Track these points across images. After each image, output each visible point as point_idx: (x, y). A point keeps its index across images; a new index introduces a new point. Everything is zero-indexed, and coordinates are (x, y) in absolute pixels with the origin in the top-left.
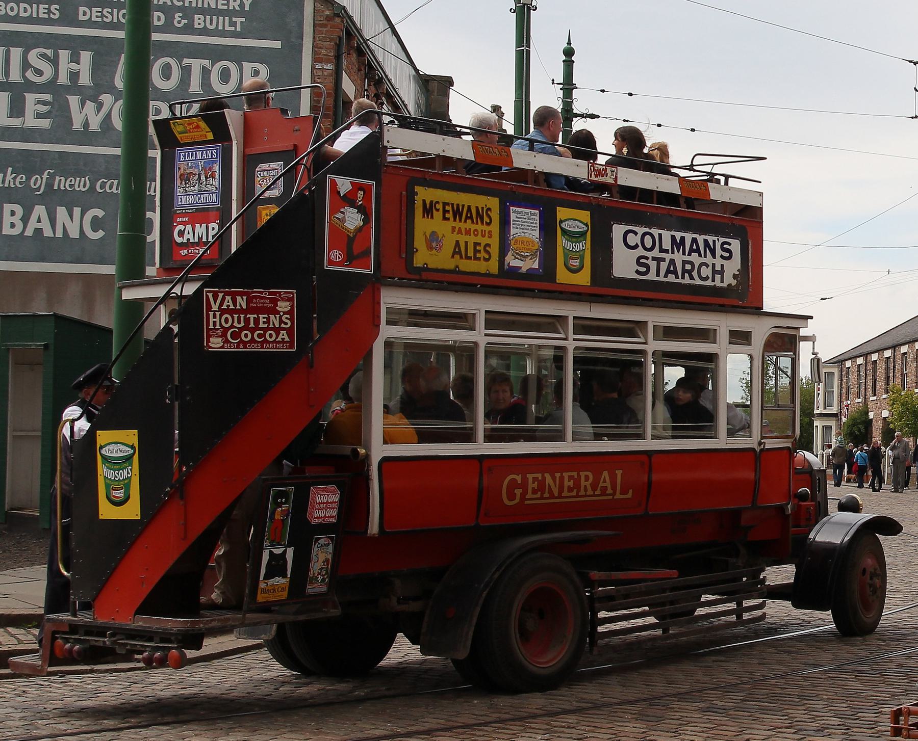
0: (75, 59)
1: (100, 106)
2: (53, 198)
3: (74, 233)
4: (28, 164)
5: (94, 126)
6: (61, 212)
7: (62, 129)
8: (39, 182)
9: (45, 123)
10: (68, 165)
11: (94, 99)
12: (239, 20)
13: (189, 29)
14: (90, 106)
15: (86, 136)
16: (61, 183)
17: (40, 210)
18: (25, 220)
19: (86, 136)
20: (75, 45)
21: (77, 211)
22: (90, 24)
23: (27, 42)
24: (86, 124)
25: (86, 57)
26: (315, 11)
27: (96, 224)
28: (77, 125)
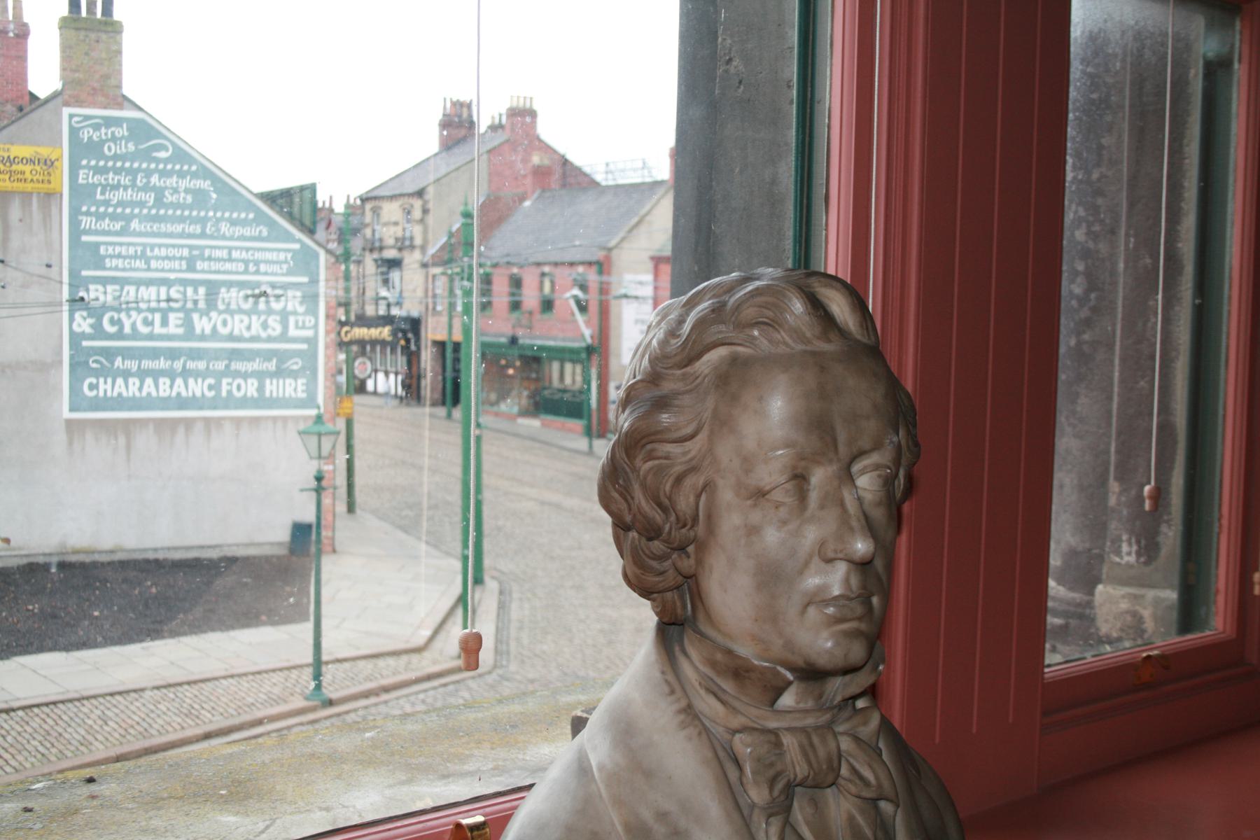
0: (196, 291)
1: (210, 319)
2: (186, 374)
3: (198, 394)
4: (173, 354)
5: (208, 331)
6: (191, 381)
7: (190, 333)
8: (178, 365)
9: (180, 331)
10: (195, 354)
11: (207, 315)
12: (285, 267)
13: (257, 272)
14: (205, 319)
15: (203, 337)
16: (191, 365)
17: (179, 381)
18: (171, 387)
19: (203, 337)
20: (196, 284)
21: (200, 380)
22: (203, 271)
23: (168, 283)
24: (203, 330)
25: (202, 291)
26: (327, 261)
27: (210, 388)
28: (198, 331)
